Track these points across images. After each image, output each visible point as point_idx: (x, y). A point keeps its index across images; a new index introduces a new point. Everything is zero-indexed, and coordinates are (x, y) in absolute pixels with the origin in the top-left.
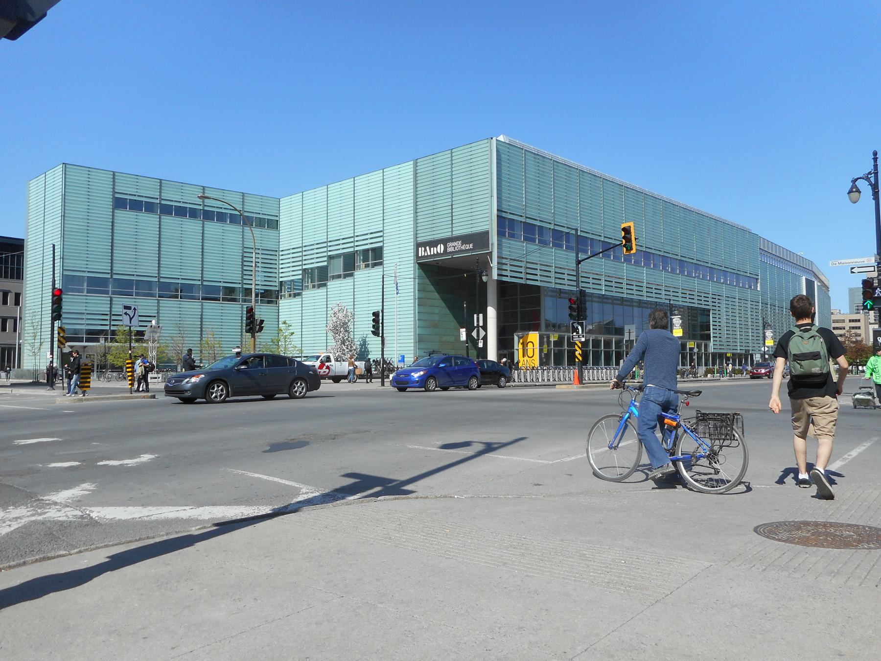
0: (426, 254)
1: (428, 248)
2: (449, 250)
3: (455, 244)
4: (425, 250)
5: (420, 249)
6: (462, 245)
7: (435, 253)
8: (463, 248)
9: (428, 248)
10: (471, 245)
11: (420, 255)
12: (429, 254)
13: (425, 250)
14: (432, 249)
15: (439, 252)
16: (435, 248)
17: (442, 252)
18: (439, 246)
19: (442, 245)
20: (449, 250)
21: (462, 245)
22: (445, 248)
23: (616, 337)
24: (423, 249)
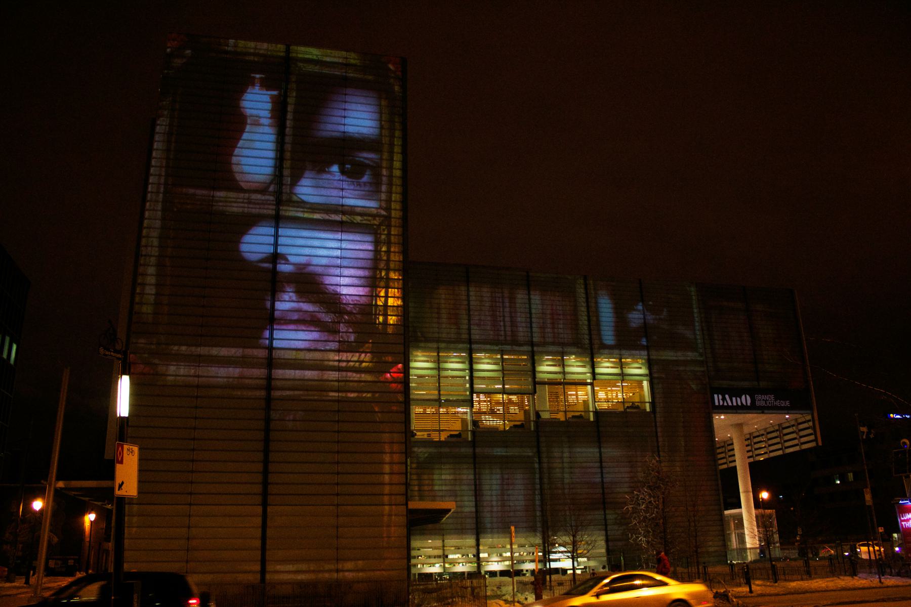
0: (725, 404)
1: (727, 396)
2: (758, 403)
3: (766, 397)
4: (724, 399)
5: (716, 396)
6: (776, 400)
7: (739, 403)
8: (777, 403)
9: (727, 396)
10: (788, 403)
11: (717, 404)
12: (730, 404)
13: (724, 399)
14: (734, 399)
15: (744, 403)
16: (738, 399)
17: (749, 404)
18: (743, 397)
19: (748, 396)
20: (758, 403)
21: (776, 400)
22: (753, 401)
23: (114, 511)
24: (720, 397)
